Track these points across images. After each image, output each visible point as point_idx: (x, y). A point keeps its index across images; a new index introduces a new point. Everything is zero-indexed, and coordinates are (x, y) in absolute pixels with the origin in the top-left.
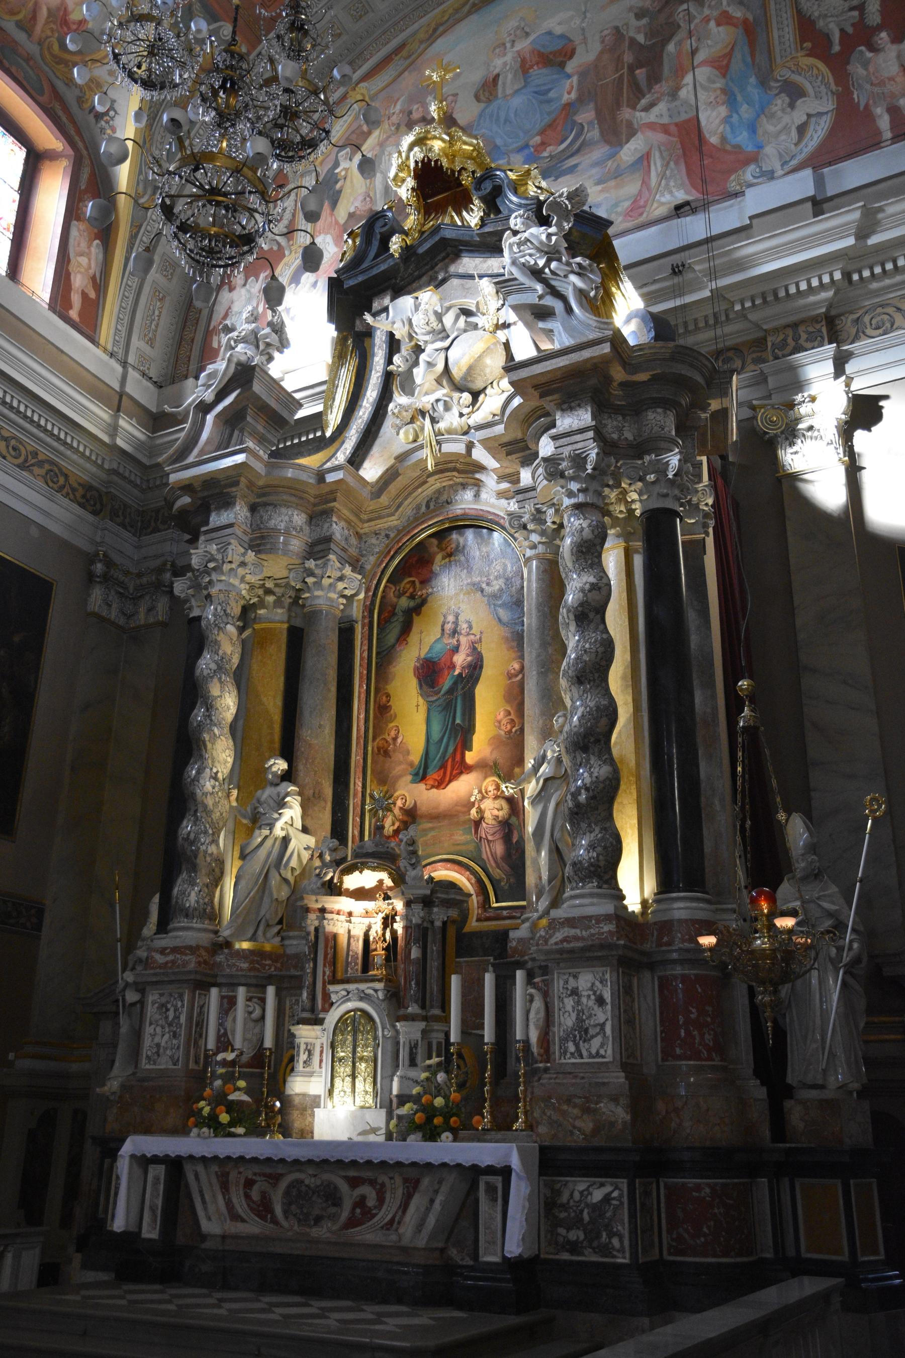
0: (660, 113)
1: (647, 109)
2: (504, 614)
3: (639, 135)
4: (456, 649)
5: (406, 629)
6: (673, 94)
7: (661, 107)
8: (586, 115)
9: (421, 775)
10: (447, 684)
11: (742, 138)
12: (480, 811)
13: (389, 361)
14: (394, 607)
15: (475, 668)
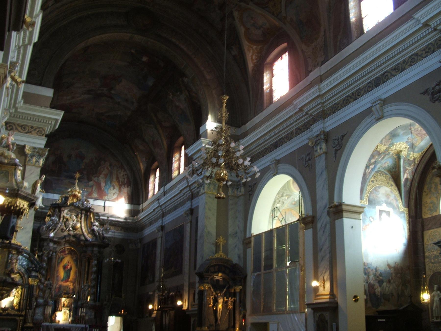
0: (96, 179)
1: (94, 177)
2: (75, 262)
3: (92, 181)
4: (68, 265)
5: (62, 260)
6: (98, 177)
7: (96, 178)
8: (85, 173)
9: (62, 281)
10: (67, 269)
11: (106, 190)
12: (70, 287)
13: (63, 219)
14: (60, 257)
15: (71, 269)
